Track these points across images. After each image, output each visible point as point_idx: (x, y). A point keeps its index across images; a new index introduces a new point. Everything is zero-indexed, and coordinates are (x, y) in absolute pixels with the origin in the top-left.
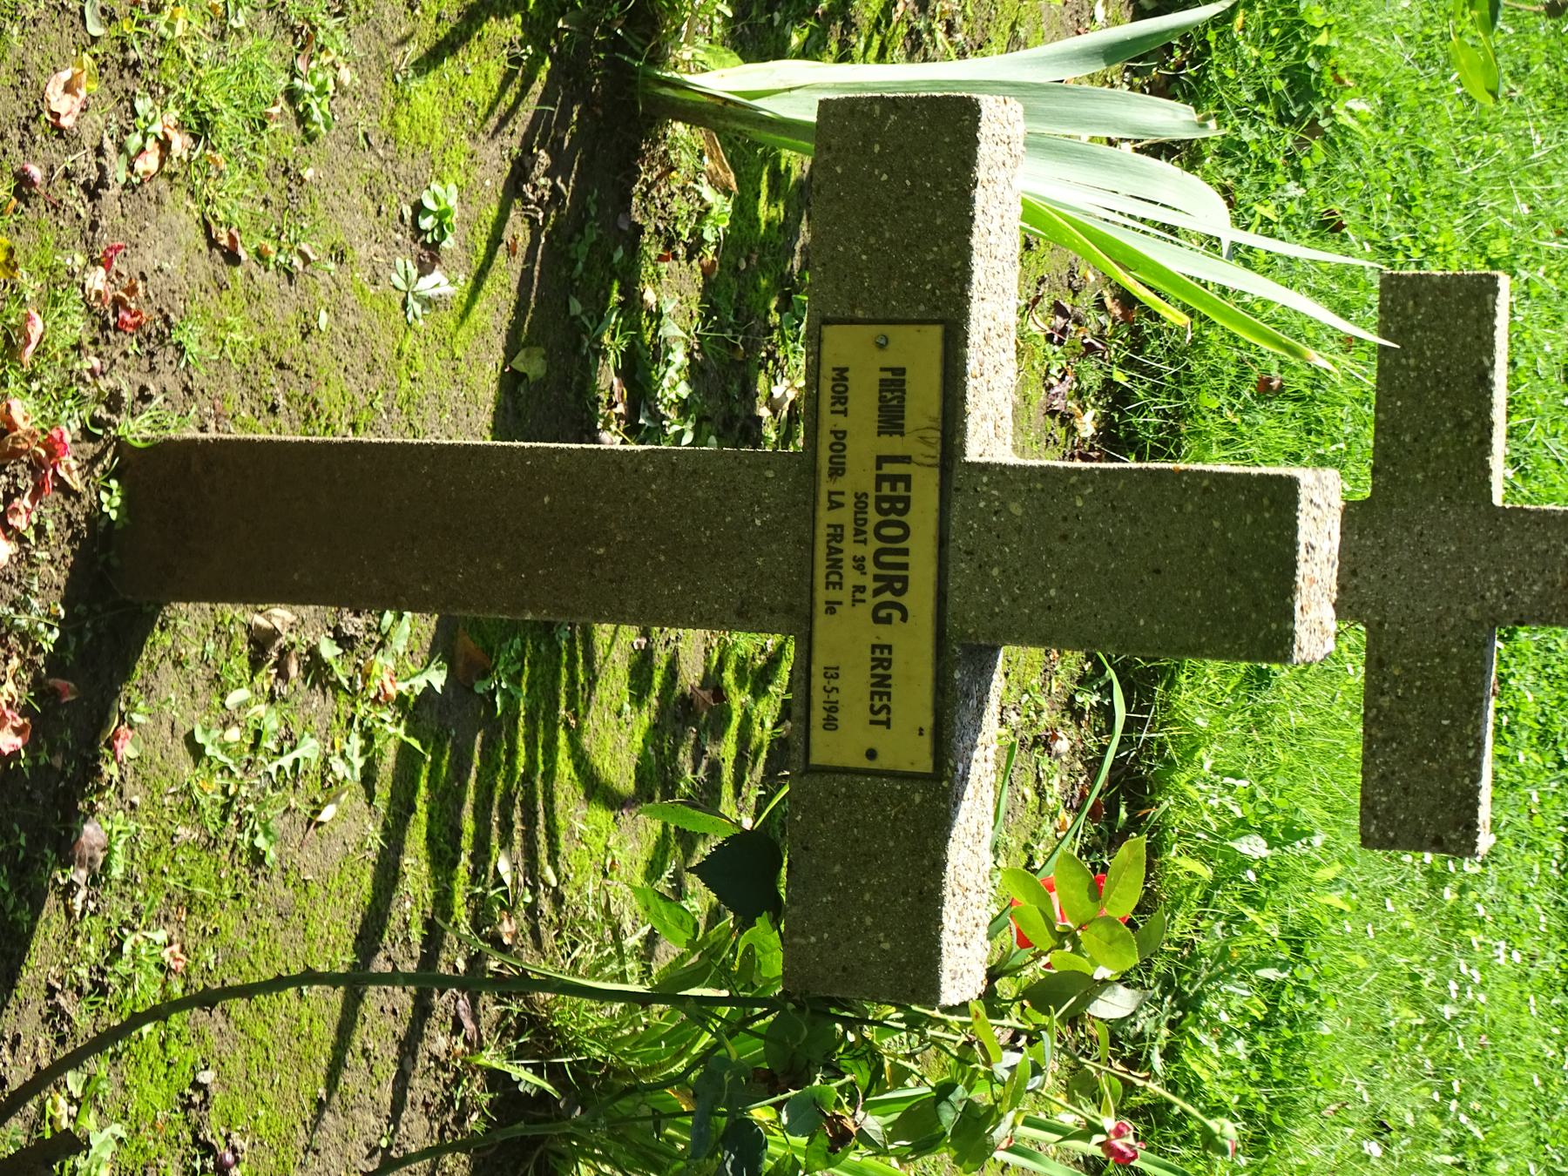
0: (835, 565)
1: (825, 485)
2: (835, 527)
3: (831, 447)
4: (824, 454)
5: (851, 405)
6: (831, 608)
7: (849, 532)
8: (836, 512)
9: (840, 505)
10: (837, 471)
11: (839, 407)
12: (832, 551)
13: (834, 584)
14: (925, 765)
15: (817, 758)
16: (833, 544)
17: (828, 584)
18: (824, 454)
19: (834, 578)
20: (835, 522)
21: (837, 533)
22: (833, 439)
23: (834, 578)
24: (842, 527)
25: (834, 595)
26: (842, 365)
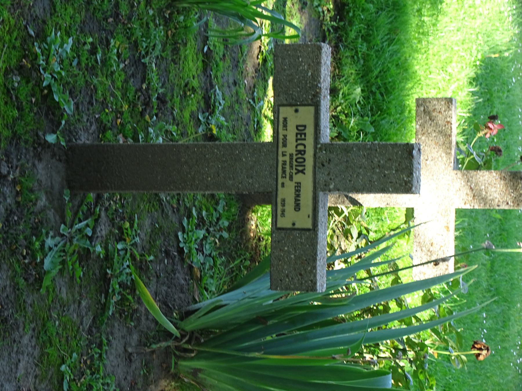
0: (284, 172)
1: (281, 150)
3: (283, 139)
4: (281, 141)
5: (288, 128)
7: (288, 163)
9: (285, 155)
10: (285, 145)
11: (285, 128)
12: (283, 168)
14: (309, 225)
16: (284, 166)
17: (282, 177)
19: (284, 175)
21: (284, 163)
23: (284, 175)
25: (284, 180)
26: (285, 116)
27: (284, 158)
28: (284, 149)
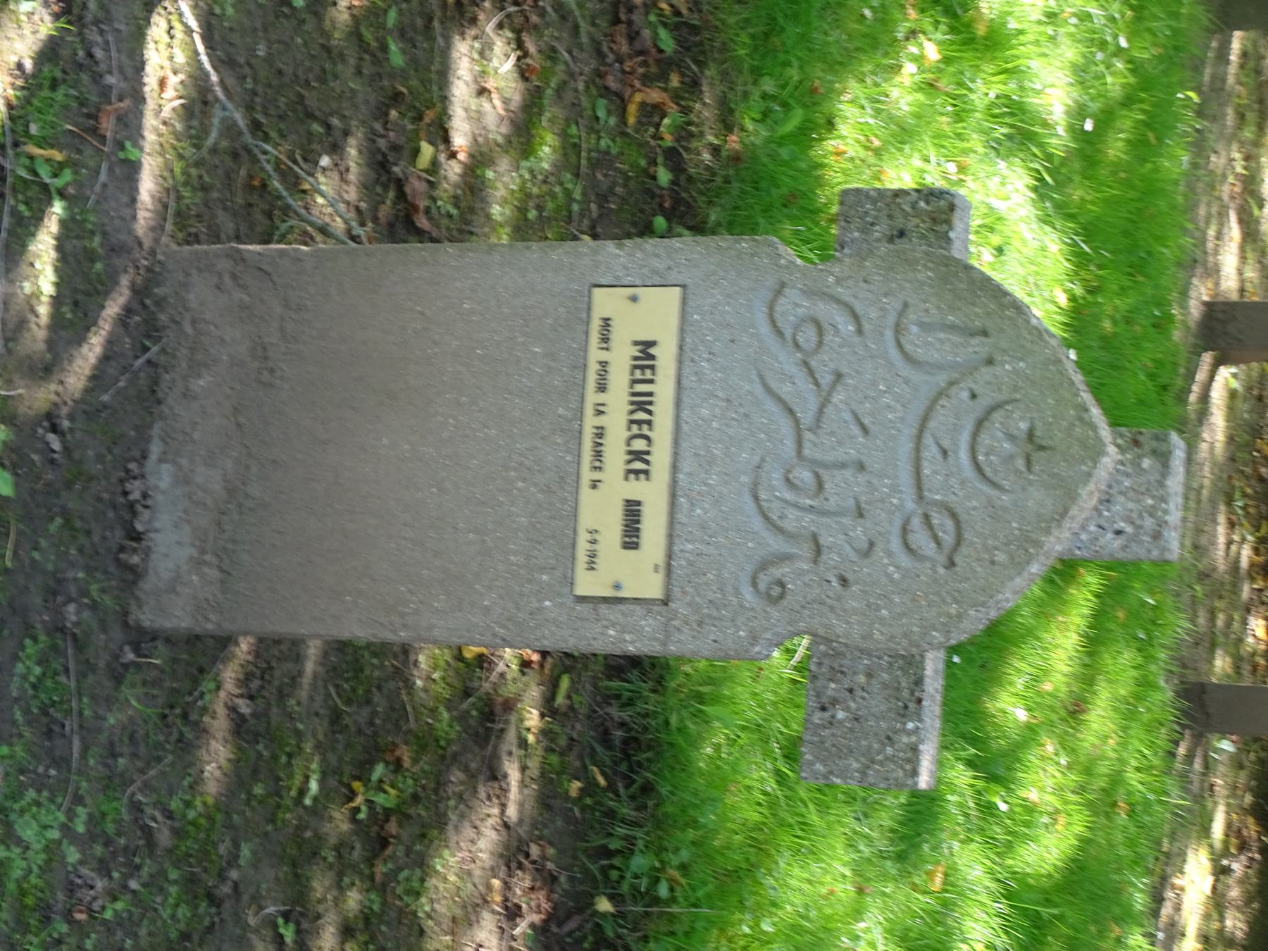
0: (598, 455)
1: (592, 397)
2: (597, 428)
4: (592, 378)
6: (594, 485)
8: (602, 417)
9: (602, 412)
10: (602, 388)
13: (596, 468)
15: (581, 590)
18: (592, 378)
19: (597, 464)
20: (599, 424)
22: (599, 367)
23: (597, 464)
24: (602, 428)
27: (600, 421)
28: (601, 398)
